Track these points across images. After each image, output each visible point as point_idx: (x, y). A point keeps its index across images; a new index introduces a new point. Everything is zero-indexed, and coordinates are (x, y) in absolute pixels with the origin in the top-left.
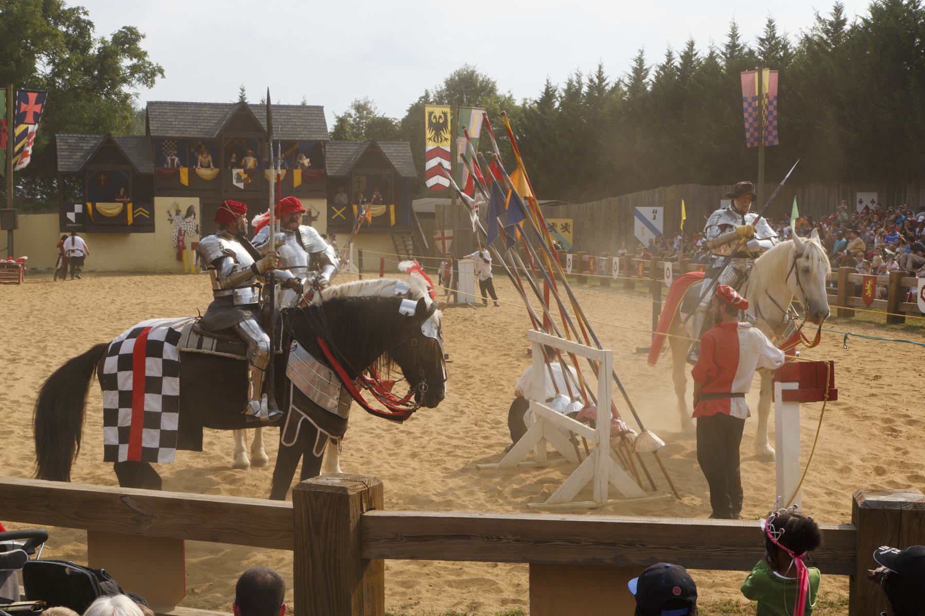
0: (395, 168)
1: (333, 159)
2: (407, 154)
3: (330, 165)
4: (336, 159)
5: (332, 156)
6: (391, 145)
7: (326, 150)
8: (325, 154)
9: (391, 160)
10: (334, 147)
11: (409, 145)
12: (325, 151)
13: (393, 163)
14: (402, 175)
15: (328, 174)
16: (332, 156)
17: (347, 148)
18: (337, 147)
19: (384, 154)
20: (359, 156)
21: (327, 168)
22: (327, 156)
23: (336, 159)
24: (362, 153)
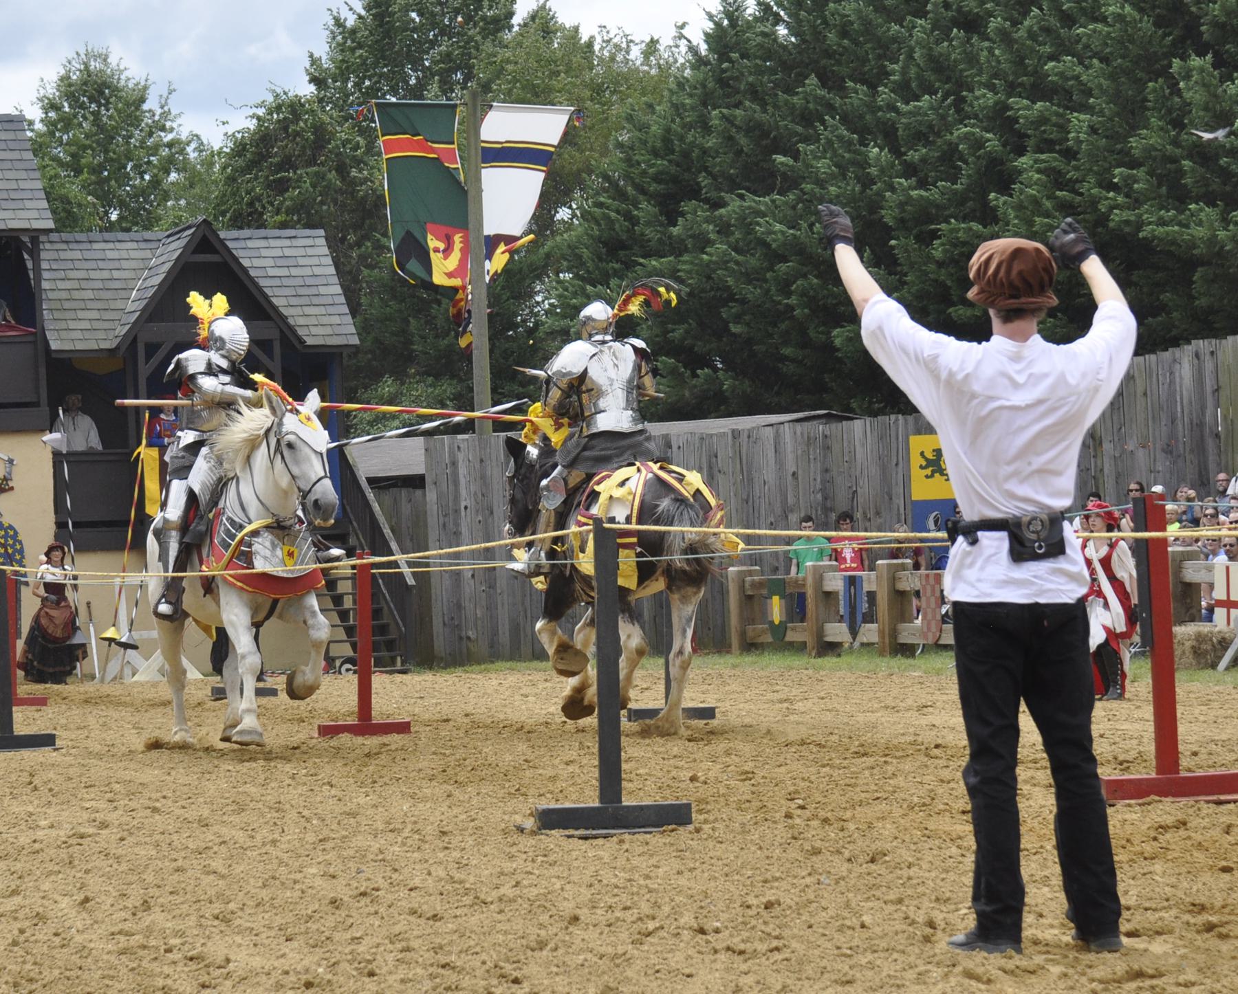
0: (283, 318)
1: (64, 295)
2: (317, 271)
3: (57, 315)
4: (76, 295)
5: (61, 285)
6: (263, 243)
7: (44, 265)
8: (39, 278)
9: (268, 292)
10: (63, 255)
11: (323, 241)
12: (37, 269)
13: (274, 300)
14: (310, 341)
15: (54, 345)
16: (61, 285)
17: (110, 255)
18: (78, 255)
19: (245, 270)
20: (157, 280)
21: (49, 325)
22: (45, 285)
23: (76, 295)
24: (168, 266)
